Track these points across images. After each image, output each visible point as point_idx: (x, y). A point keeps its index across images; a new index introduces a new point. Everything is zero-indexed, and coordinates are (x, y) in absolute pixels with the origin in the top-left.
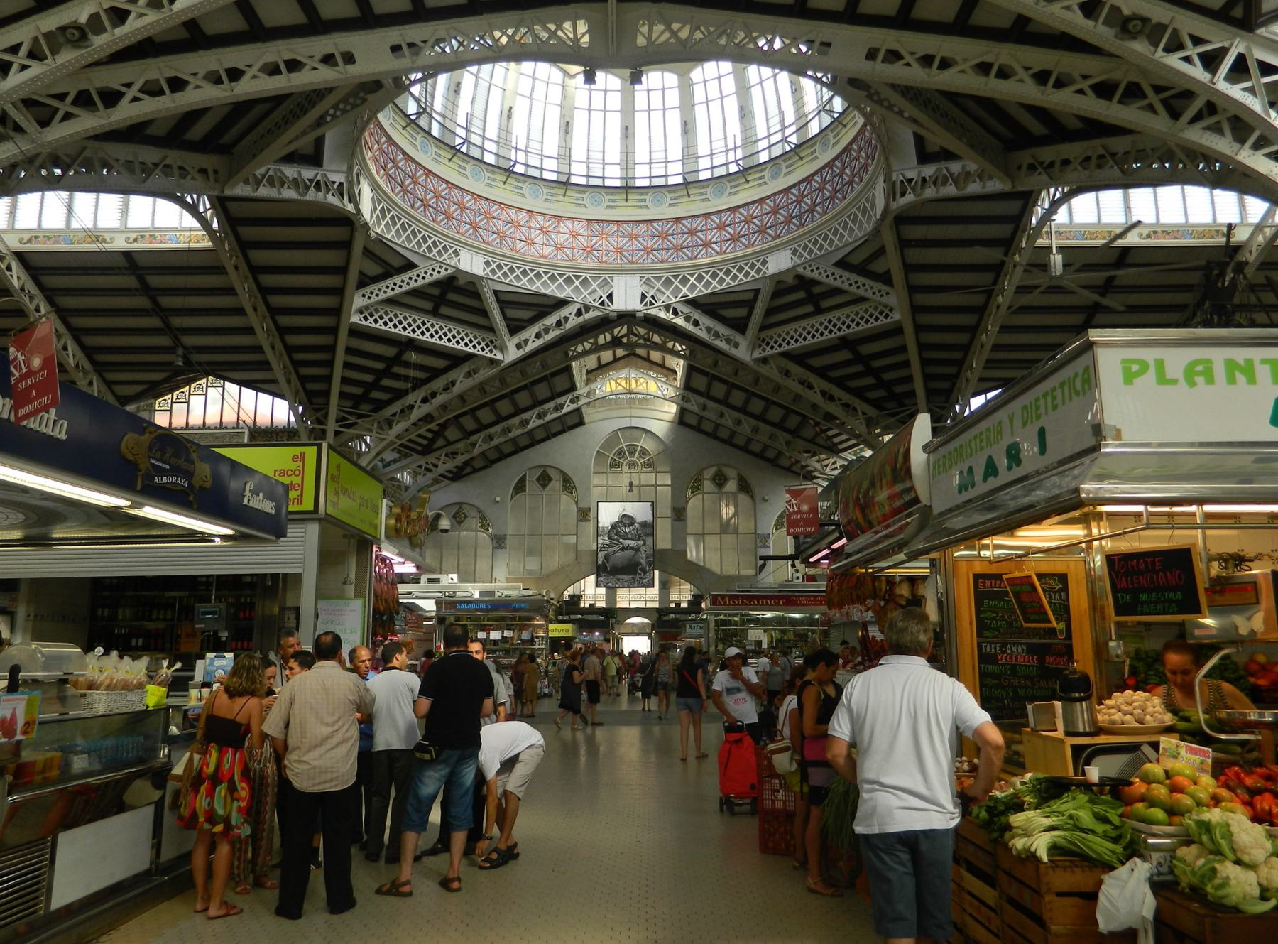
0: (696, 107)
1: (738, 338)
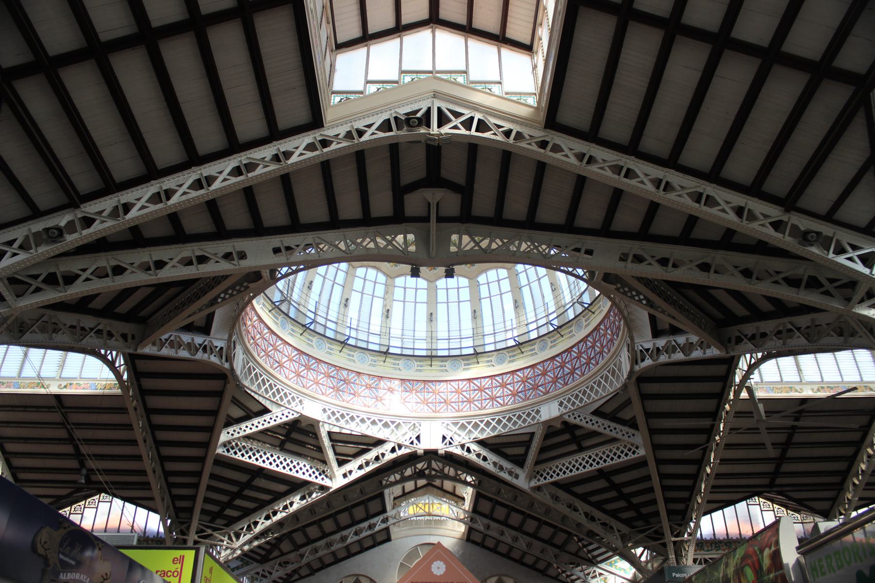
0: (482, 300)
1: (518, 471)
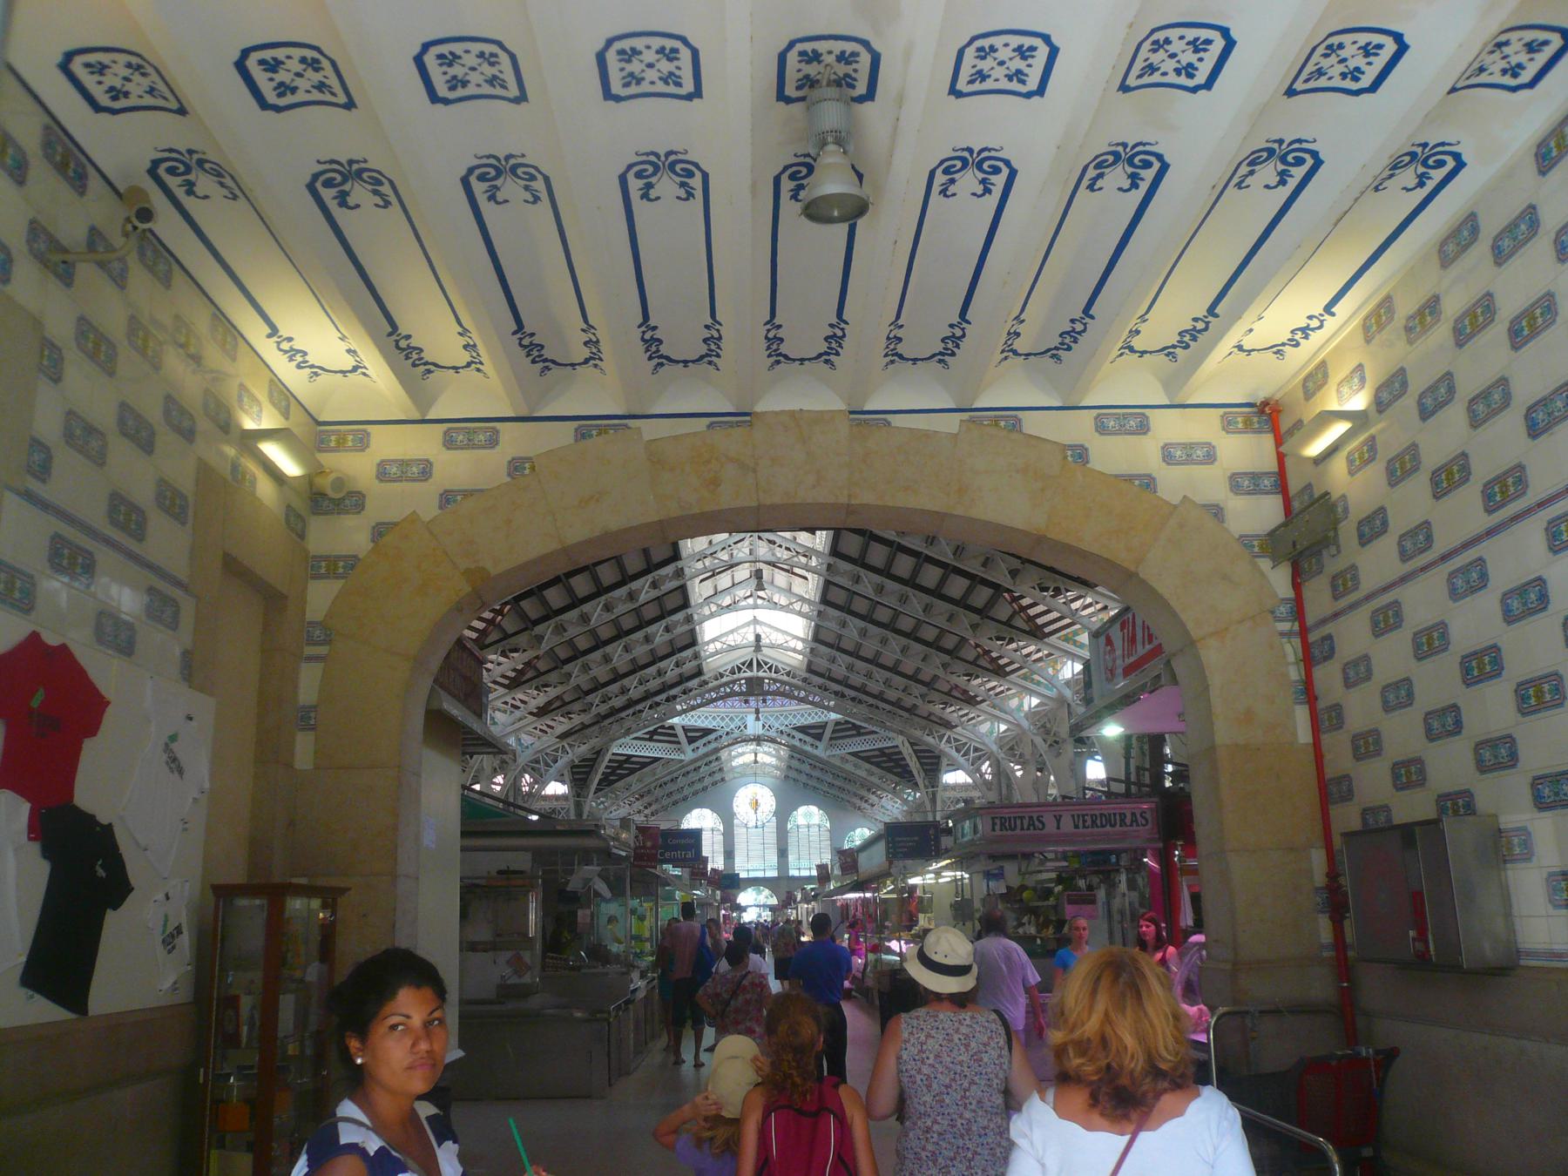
1: (818, 743)
